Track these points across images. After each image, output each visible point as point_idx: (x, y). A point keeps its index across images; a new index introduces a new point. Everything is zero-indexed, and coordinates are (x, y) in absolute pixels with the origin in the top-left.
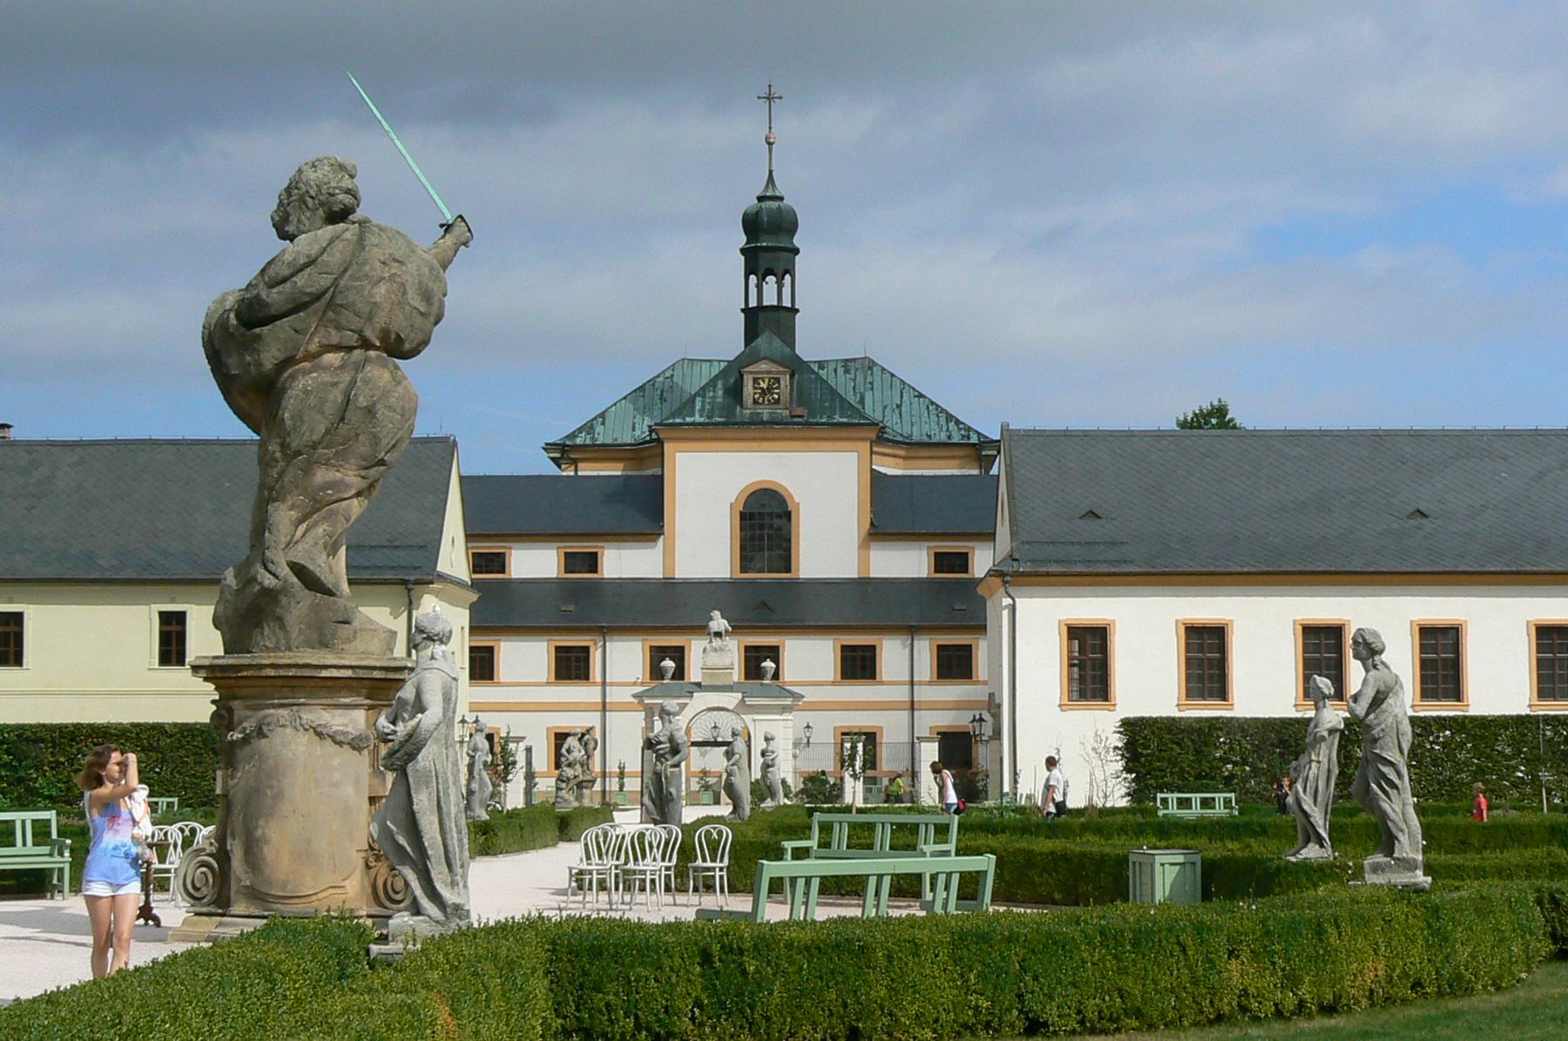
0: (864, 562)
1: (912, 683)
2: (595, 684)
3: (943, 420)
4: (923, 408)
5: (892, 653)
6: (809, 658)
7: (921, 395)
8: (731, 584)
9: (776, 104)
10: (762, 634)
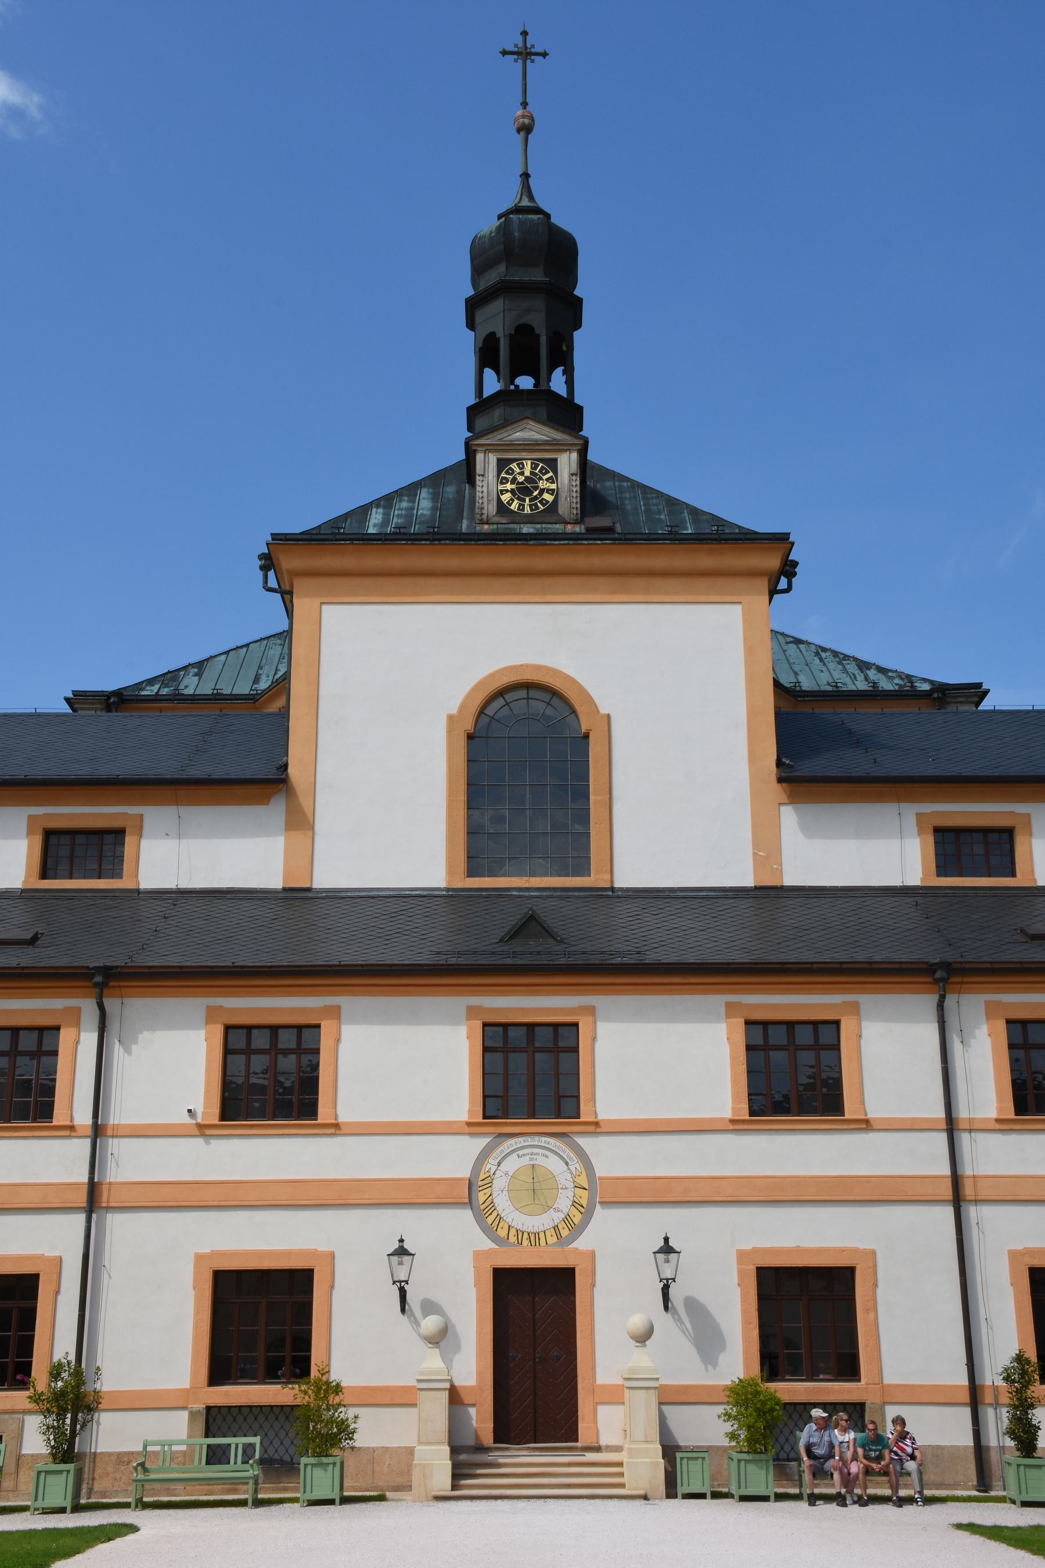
0: (766, 844)
1: (951, 1126)
2: (71, 1129)
3: (852, 668)
4: (810, 656)
5: (890, 1048)
6: (663, 1061)
7: (798, 641)
8: (452, 896)
9: (535, 67)
10: (533, 989)
